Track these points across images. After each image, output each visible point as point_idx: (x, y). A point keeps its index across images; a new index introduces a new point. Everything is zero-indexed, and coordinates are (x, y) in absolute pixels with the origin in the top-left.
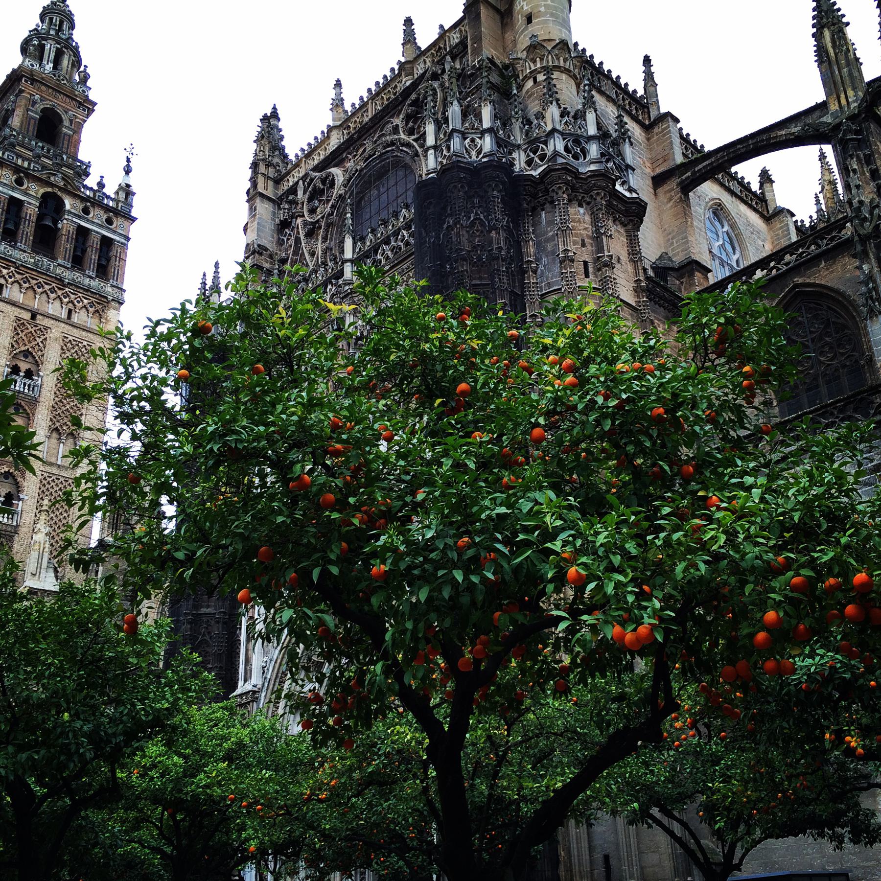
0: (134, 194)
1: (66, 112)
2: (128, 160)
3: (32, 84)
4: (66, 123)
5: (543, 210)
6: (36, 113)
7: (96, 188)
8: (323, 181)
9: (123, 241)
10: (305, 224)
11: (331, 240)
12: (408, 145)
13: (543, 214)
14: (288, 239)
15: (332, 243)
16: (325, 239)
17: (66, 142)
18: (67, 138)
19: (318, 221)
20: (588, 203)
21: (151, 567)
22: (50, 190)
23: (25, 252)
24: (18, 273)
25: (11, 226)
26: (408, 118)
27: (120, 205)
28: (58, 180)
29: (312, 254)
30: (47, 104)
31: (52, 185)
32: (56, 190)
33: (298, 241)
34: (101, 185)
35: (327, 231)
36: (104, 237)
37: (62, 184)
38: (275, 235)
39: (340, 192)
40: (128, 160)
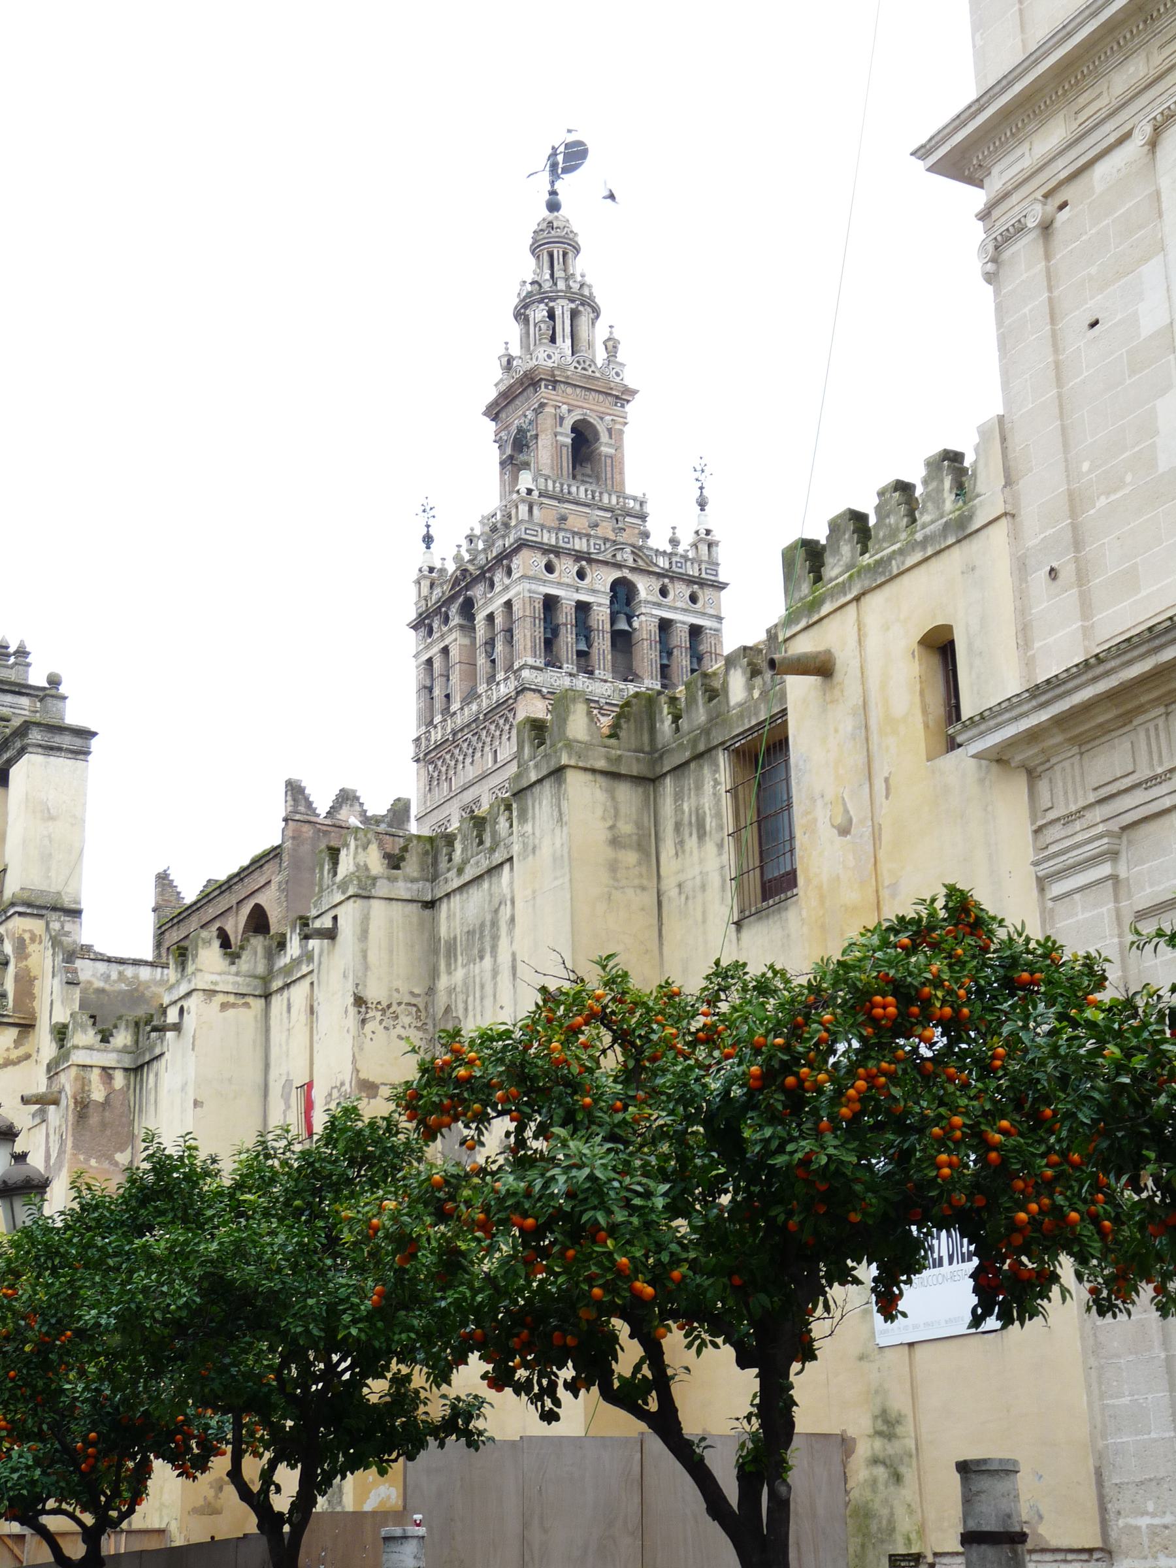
0: (717, 544)
1: (602, 419)
3: (554, 388)
4: (604, 437)
6: (567, 436)
7: (669, 549)
17: (609, 469)
18: (609, 461)
22: (616, 574)
23: (606, 681)
24: (603, 715)
25: (583, 647)
28: (627, 557)
30: (576, 416)
31: (618, 566)
32: (626, 573)
34: (674, 542)
37: (630, 563)
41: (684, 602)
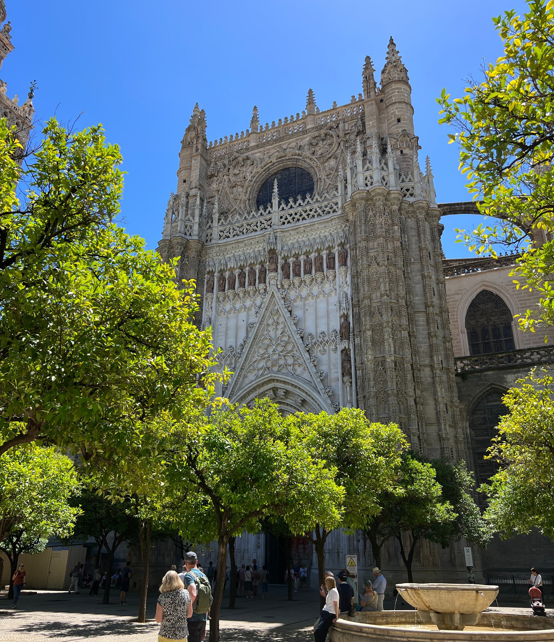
2: (32, 90)
40: (32, 90)
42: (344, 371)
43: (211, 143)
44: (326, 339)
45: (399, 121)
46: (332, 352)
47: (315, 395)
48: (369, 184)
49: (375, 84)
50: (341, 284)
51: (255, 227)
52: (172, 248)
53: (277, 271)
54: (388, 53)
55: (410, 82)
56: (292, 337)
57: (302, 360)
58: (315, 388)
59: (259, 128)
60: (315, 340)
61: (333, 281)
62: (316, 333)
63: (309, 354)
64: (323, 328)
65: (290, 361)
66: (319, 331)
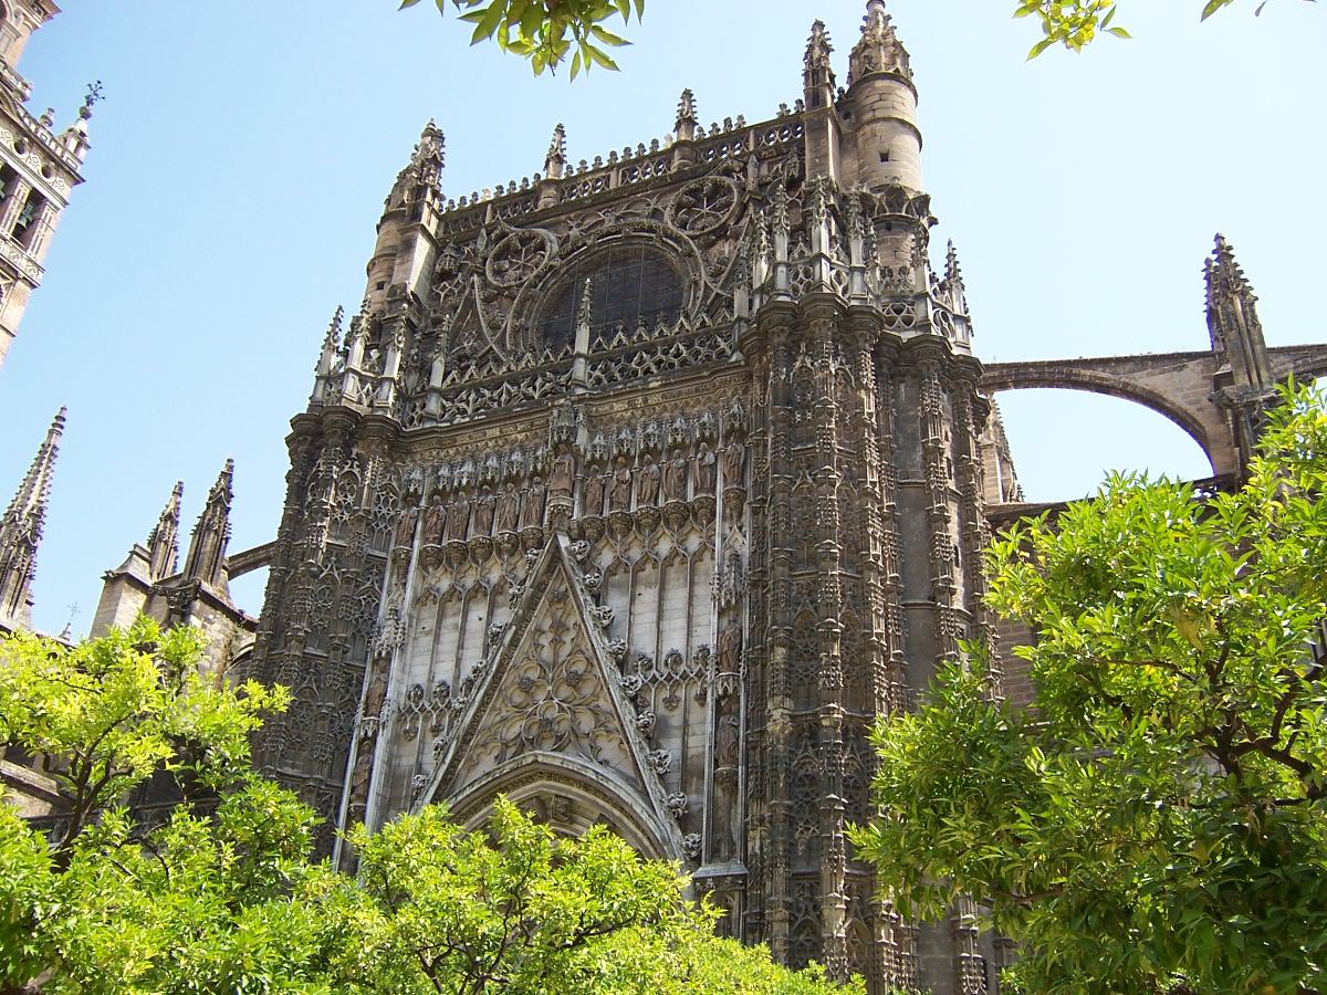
5: (901, 382)
7: (39, 121)
8: (524, 241)
9: (59, 205)
10: (485, 285)
11: (528, 318)
12: (677, 239)
13: (902, 386)
14: (446, 295)
15: (530, 324)
16: (518, 315)
19: (508, 288)
20: (951, 391)
21: (434, 723)
26: (679, 207)
27: (67, 155)
29: (494, 327)
33: (470, 303)
35: (522, 303)
36: (34, 189)
38: (428, 284)
39: (551, 263)
40: (90, 102)
41: (38, 168)
42: (719, 754)
43: (451, 202)
44: (683, 668)
45: (885, 157)
46: (695, 705)
47: (639, 807)
48: (801, 287)
49: (832, 77)
50: (727, 531)
51: (530, 389)
52: (321, 434)
53: (572, 496)
54: (865, 18)
55: (914, 80)
56: (595, 662)
57: (616, 722)
58: (644, 794)
59: (565, 171)
60: (654, 671)
61: (709, 522)
62: (658, 651)
63: (636, 707)
64: (675, 641)
65: (587, 722)
66: (666, 650)
